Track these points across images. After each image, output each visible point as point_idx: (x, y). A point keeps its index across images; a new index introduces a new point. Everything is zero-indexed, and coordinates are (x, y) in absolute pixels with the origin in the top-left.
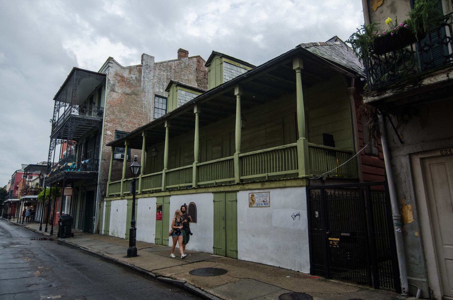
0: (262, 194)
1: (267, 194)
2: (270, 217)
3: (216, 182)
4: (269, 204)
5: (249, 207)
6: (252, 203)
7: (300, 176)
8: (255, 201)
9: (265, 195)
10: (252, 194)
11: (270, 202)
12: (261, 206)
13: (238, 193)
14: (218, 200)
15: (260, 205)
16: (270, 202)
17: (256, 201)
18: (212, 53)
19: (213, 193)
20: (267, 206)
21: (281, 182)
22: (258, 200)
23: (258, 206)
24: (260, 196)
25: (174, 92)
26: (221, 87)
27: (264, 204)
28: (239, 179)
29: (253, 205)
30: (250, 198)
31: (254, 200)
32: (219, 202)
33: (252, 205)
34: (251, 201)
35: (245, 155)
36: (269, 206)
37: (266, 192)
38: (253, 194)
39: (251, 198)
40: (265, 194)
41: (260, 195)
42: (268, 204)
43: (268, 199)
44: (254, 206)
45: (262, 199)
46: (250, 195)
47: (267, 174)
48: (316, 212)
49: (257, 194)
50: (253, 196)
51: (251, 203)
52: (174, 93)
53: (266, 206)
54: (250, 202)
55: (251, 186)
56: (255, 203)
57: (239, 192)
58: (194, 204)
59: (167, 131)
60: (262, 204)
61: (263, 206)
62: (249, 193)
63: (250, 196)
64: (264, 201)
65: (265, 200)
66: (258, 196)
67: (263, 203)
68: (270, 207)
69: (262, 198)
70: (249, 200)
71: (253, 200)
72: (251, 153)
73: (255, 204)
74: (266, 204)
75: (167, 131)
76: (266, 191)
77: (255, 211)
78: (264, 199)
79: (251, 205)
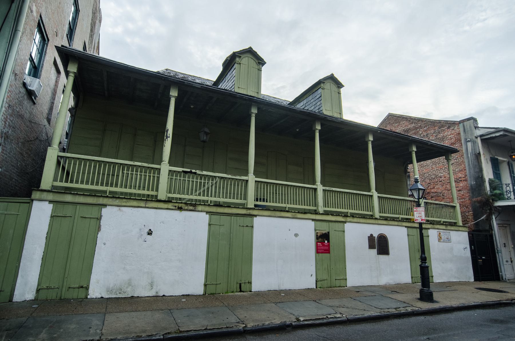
5: (439, 242)
6: (440, 239)
14: (412, 234)
18: (249, 48)
19: (406, 227)
20: (450, 242)
38: (440, 232)
39: (439, 235)
43: (449, 237)
44: (441, 241)
45: (446, 237)
50: (440, 234)
55: (438, 226)
58: (385, 236)
63: (438, 234)
65: (448, 238)
69: (446, 236)
72: (355, 192)
73: (442, 240)
74: (449, 240)
76: (448, 231)
78: (447, 237)
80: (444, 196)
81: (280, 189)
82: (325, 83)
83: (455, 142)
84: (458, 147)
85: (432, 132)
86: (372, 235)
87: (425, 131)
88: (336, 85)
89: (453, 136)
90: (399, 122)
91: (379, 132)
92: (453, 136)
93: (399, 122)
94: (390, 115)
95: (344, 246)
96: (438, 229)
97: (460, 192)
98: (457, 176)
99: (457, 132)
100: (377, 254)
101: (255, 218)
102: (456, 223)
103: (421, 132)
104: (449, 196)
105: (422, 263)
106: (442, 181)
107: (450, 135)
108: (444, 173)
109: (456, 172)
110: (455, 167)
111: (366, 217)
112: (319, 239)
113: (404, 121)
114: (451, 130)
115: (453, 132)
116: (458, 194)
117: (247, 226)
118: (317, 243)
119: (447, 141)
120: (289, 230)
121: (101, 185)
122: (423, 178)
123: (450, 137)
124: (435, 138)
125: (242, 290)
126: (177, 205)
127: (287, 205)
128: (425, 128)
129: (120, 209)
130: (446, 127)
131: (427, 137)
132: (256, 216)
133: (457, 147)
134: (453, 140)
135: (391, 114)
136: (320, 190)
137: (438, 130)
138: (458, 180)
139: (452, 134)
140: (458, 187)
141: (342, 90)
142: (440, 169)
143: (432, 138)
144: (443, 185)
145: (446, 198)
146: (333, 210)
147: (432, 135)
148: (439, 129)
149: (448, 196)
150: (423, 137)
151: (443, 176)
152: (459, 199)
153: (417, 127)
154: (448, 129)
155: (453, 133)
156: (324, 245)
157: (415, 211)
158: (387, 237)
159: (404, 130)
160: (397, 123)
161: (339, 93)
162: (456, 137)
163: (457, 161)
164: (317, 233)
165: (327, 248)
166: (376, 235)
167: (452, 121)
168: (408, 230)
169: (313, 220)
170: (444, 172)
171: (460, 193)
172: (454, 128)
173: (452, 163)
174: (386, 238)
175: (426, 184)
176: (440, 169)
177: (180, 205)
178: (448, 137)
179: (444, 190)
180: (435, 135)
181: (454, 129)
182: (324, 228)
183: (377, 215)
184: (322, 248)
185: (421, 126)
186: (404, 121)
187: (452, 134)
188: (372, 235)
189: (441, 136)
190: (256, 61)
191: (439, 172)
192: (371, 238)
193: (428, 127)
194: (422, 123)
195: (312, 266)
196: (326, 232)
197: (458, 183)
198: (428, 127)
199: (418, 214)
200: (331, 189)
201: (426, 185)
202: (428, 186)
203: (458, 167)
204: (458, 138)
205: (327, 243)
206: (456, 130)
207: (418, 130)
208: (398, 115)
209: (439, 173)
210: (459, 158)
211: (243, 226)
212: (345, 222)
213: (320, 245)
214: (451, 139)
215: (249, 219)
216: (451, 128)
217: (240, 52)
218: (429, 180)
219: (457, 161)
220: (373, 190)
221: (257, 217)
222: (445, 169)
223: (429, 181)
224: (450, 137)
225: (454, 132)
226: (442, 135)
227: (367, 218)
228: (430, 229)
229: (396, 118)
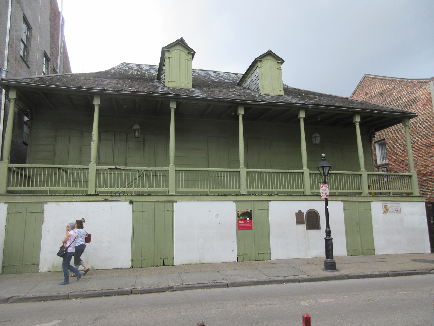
3: (50, 189)
4: (400, 212)
5: (384, 214)
6: (386, 211)
7: (170, 194)
11: (400, 211)
13: (371, 203)
14: (350, 208)
17: (389, 210)
19: (342, 201)
22: (391, 209)
24: (392, 206)
27: (397, 212)
30: (383, 208)
34: (385, 210)
36: (400, 213)
37: (397, 204)
38: (386, 204)
39: (385, 207)
41: (392, 206)
43: (399, 209)
44: (388, 213)
45: (394, 209)
46: (384, 205)
48: (431, 217)
51: (384, 211)
53: (398, 213)
55: (384, 198)
56: (389, 211)
58: (316, 212)
60: (394, 212)
63: (384, 206)
65: (397, 210)
67: (395, 211)
70: (383, 209)
71: (386, 209)
74: (398, 212)
76: (397, 203)
77: (388, 217)
78: (396, 208)
79: (384, 213)
80: (417, 163)
82: (262, 61)
83: (427, 103)
84: (430, 109)
85: (405, 93)
86: (300, 211)
87: (399, 92)
88: (275, 61)
89: (425, 96)
90: (374, 84)
91: (310, 108)
92: (425, 96)
93: (374, 84)
94: (366, 77)
97: (432, 159)
98: (429, 140)
99: (429, 92)
101: (175, 204)
102: (412, 193)
103: (395, 94)
104: (423, 163)
105: (327, 236)
106: (414, 147)
107: (422, 95)
108: (417, 139)
109: (427, 136)
110: (427, 131)
111: (293, 195)
112: (240, 217)
113: (378, 82)
114: (422, 89)
115: (425, 92)
116: (430, 160)
117: (168, 211)
118: (238, 221)
119: (419, 103)
120: (210, 212)
121: (39, 186)
122: (397, 145)
123: (421, 97)
124: (408, 100)
125: (165, 264)
126: (104, 197)
127: (209, 189)
128: (398, 89)
129: (58, 204)
130: (418, 86)
131: (400, 99)
132: (176, 201)
133: (428, 108)
134: (424, 101)
135: (366, 76)
136: (243, 173)
137: (410, 90)
138: (430, 145)
139: (424, 94)
140: (430, 153)
141: (283, 66)
142: (413, 134)
143: (404, 99)
144: (416, 151)
145: (419, 165)
147: (404, 97)
148: (412, 89)
149: (421, 164)
150: (396, 100)
151: (415, 141)
152: (431, 166)
153: (391, 88)
154: (420, 88)
155: (424, 93)
156: (245, 222)
157: (321, 188)
158: (317, 212)
159: (379, 92)
160: (372, 85)
161: (280, 69)
162: (427, 97)
163: (429, 124)
164: (239, 212)
165: (249, 225)
166: (304, 211)
167: (423, 79)
168: (344, 204)
170: (416, 137)
171: (432, 160)
172: (426, 87)
173: (424, 126)
174: (317, 214)
175: (401, 152)
176: (413, 134)
177: (106, 197)
178: (419, 98)
179: (417, 157)
180: (407, 97)
181: (425, 88)
182: (245, 208)
183: (308, 191)
184: (244, 224)
185: (394, 87)
186: (378, 82)
187: (424, 94)
188: (300, 211)
189: (414, 96)
190: (185, 52)
191: (412, 137)
192: (299, 215)
193: (401, 87)
194: (395, 83)
195: (233, 242)
196: (248, 210)
197: (430, 149)
198: (401, 87)
199: (323, 190)
201: (400, 152)
202: (403, 153)
203: (430, 131)
204: (429, 98)
205: (249, 220)
206: (428, 89)
207: (392, 91)
208: (373, 76)
209: (412, 138)
210: (431, 121)
212: (270, 201)
213: (241, 222)
214: (423, 100)
215: (169, 204)
216: (423, 87)
217: (168, 47)
218: (403, 146)
219: (429, 124)
220: (305, 168)
221: (177, 202)
222: (417, 134)
223: (403, 148)
224: (421, 97)
225: (426, 92)
226: (414, 96)
228: (373, 202)
229: (371, 79)
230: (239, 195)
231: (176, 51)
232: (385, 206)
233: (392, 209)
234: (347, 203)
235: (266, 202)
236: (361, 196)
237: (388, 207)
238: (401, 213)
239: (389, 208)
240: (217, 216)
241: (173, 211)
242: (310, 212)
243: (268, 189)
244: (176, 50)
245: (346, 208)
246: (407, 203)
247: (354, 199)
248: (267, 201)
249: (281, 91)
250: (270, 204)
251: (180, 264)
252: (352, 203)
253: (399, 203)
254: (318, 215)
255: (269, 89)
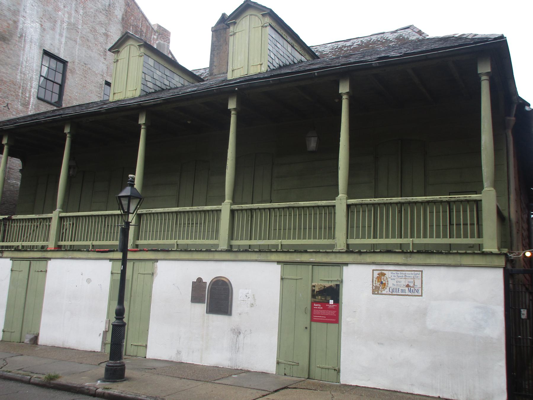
0: (406, 274)
1: (416, 274)
2: (423, 313)
5: (373, 294)
8: (386, 285)
9: (413, 275)
10: (379, 272)
12: (400, 293)
13: (345, 268)
15: (400, 291)
16: (423, 288)
19: (279, 262)
20: (416, 294)
21: (451, 257)
22: (395, 283)
23: (394, 293)
24: (398, 277)
25: (131, 55)
26: (314, 73)
27: (410, 291)
28: (345, 242)
29: (381, 291)
30: (374, 279)
31: (384, 282)
32: (295, 280)
33: (379, 290)
34: (378, 284)
35: (364, 202)
37: (414, 271)
38: (383, 272)
39: (379, 278)
40: (412, 274)
41: (399, 275)
42: (418, 291)
43: (418, 283)
44: (383, 292)
45: (404, 282)
46: (376, 274)
47: (411, 239)
48: (522, 310)
49: (391, 273)
51: (376, 287)
52: (131, 59)
53: (413, 294)
54: (374, 285)
55: (379, 258)
56: (388, 288)
57: (348, 266)
59: (143, 132)
60: (402, 291)
61: (406, 294)
62: (373, 270)
64: (408, 286)
65: (411, 285)
66: (395, 276)
68: (422, 296)
70: (373, 282)
71: (382, 283)
73: (387, 290)
75: (143, 132)
79: (376, 291)
81: (182, 219)
86: (200, 280)
91: (236, 89)
95: (151, 297)
96: (374, 263)
100: (207, 313)
117: (41, 271)
132: (50, 259)
146: (167, 243)
166: (207, 279)
169: (111, 260)
188: (200, 280)
195: (102, 322)
200: (150, 212)
211: (38, 271)
212: (156, 260)
227: (83, 251)
230: (116, 250)
231: (126, 48)
232: (378, 274)
233: (398, 284)
234: (288, 267)
235: (149, 264)
236: (333, 252)
237: (387, 279)
238: (422, 293)
239: (389, 280)
240: (89, 281)
241: (46, 271)
242: (216, 281)
243: (150, 241)
244: (126, 47)
245: (286, 277)
246: (443, 271)
247: (305, 258)
248: (152, 261)
249: (263, 65)
250: (160, 265)
251: (43, 345)
252: (299, 267)
253: (420, 268)
254: (230, 288)
255: (243, 67)
